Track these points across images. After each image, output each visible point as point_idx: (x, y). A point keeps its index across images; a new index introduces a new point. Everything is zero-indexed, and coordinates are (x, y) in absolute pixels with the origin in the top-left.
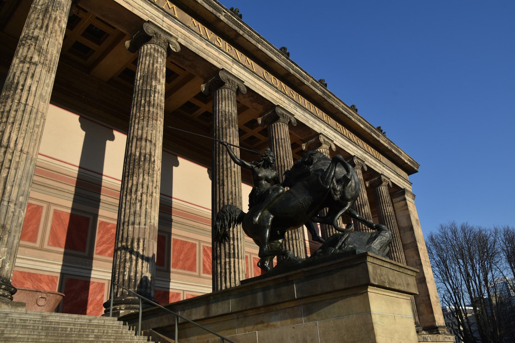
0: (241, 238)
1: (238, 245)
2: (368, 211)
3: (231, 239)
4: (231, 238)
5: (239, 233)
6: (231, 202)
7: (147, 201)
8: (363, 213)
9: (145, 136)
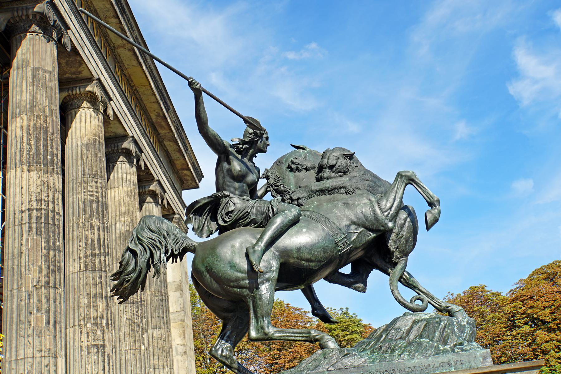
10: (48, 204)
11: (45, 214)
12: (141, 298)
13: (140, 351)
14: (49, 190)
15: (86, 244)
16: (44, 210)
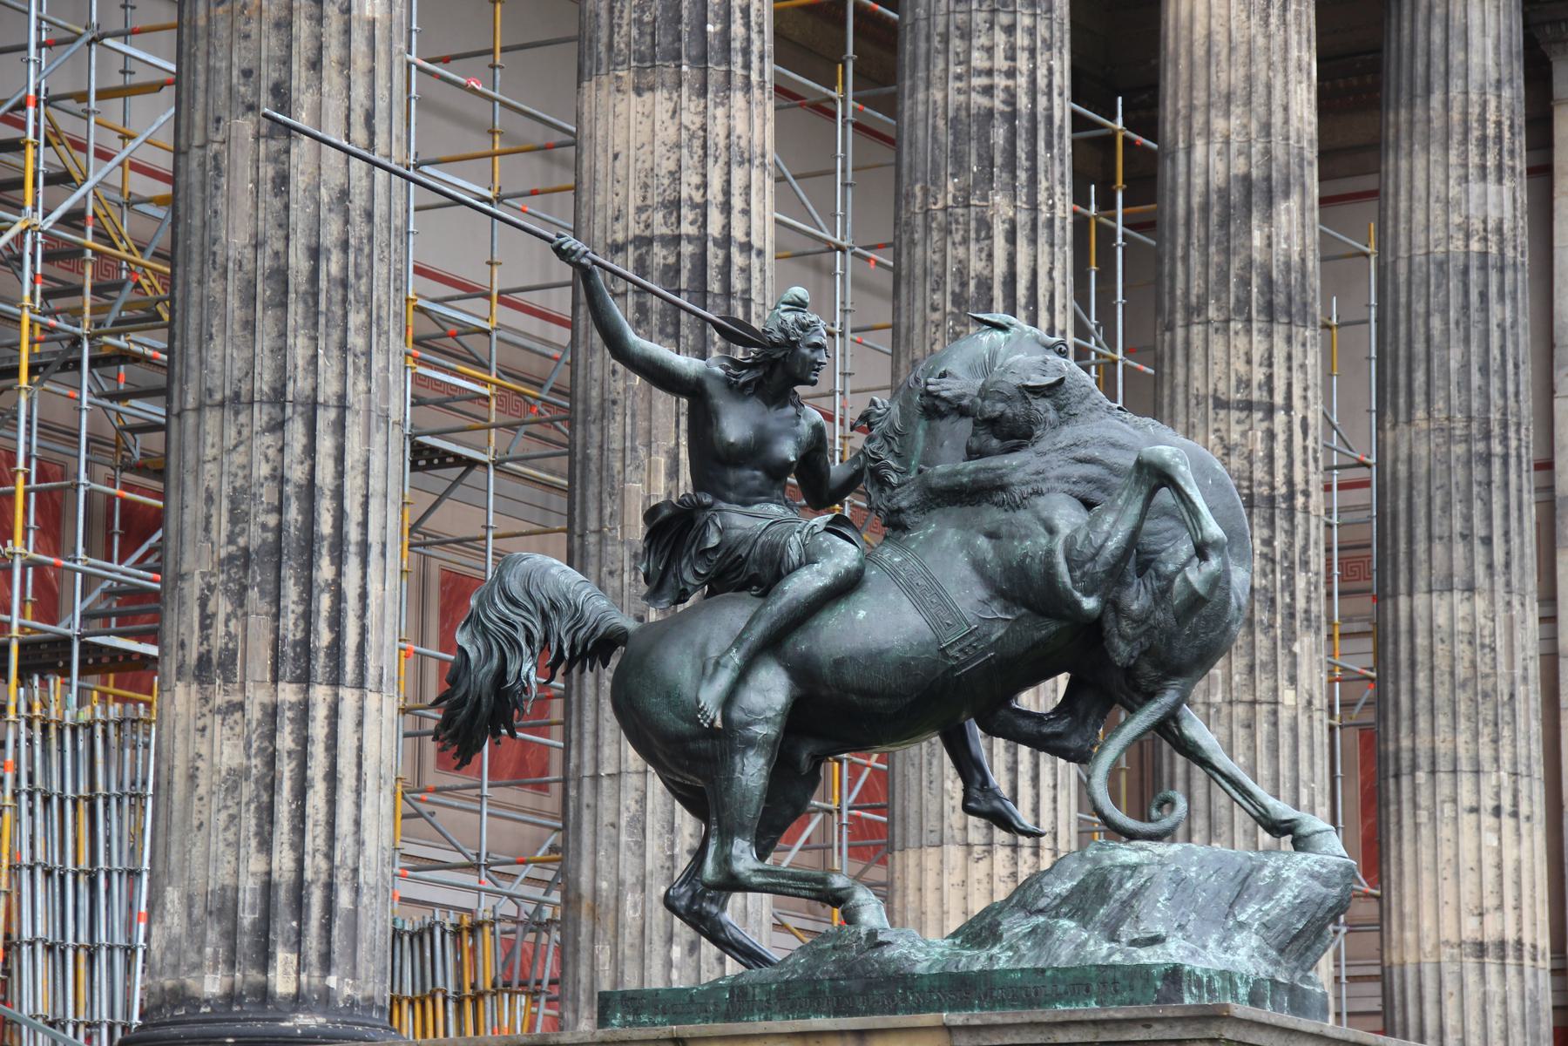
0: (384, 545)
1: (363, 596)
2: (1296, 248)
3: (325, 551)
4: (322, 538)
5: (374, 505)
6: (335, 269)
8: (1257, 256)
10: (705, 216)
11: (692, 256)
12: (1290, 482)
13: (1275, 713)
14: (710, 161)
15: (959, 300)
16: (690, 239)
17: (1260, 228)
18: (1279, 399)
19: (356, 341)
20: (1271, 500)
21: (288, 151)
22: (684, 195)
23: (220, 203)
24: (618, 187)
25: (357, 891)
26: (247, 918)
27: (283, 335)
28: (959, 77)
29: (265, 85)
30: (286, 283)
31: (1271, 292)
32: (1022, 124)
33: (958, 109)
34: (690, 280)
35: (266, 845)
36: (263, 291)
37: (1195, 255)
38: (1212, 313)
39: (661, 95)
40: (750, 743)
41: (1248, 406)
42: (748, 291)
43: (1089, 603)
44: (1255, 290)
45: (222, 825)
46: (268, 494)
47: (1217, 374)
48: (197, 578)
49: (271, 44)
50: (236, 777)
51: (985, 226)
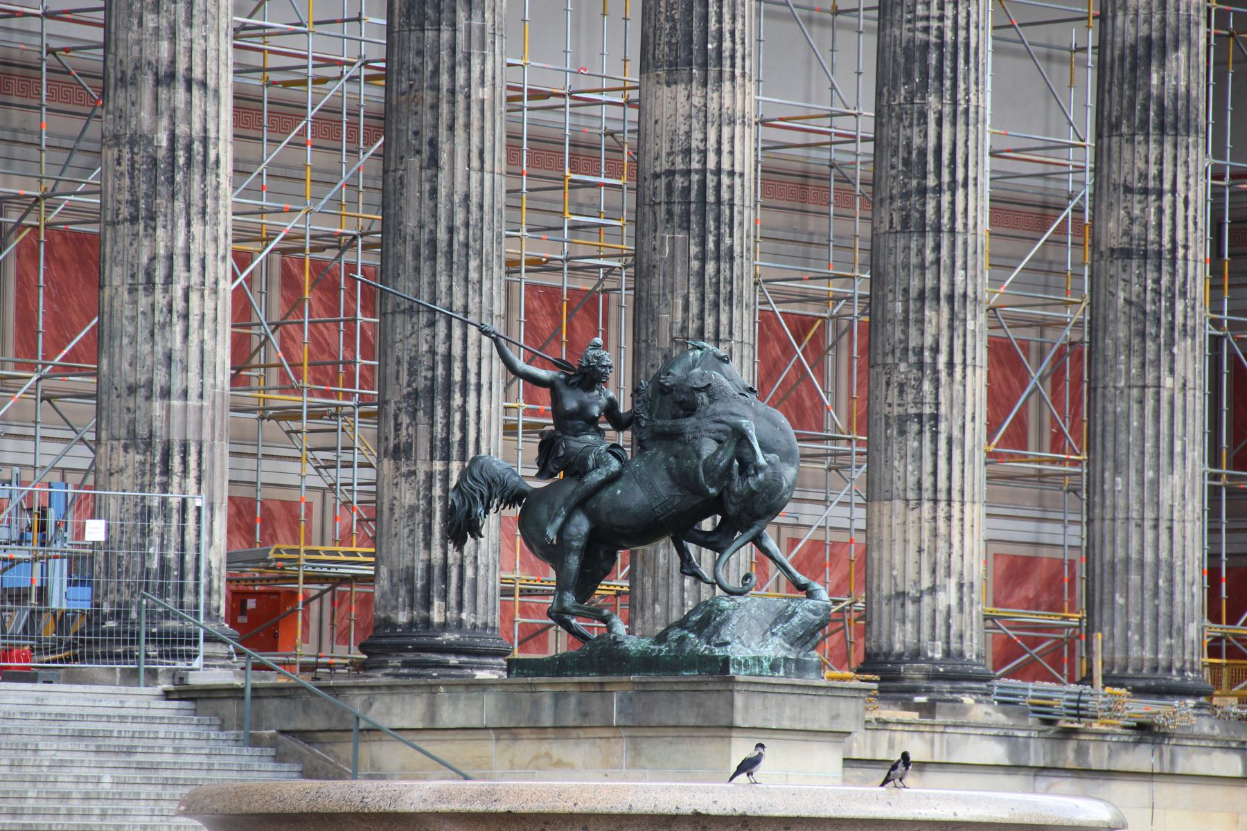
1: (479, 412)
2: (1183, 83)
6: (462, 237)
7: (203, 315)
8: (1154, 91)
9: (186, 66)
10: (705, 157)
11: (698, 181)
12: (1173, 240)
13: (1158, 393)
14: (709, 125)
15: (907, 162)
16: (697, 171)
17: (1158, 72)
18: (1167, 186)
19: (473, 275)
20: (1159, 254)
21: (436, 176)
22: (693, 146)
23: (403, 202)
24: (658, 140)
25: (476, 568)
26: (419, 584)
27: (434, 275)
28: (909, 21)
29: (426, 140)
30: (435, 246)
31: (1163, 115)
32: (948, 50)
33: (908, 41)
34: (697, 195)
35: (428, 546)
36: (425, 251)
37: (1115, 89)
38: (1124, 129)
39: (681, 87)
40: (571, 550)
41: (1145, 191)
42: (732, 199)
43: (712, 491)
44: (1152, 114)
45: (406, 535)
46: (426, 360)
47: (1126, 170)
48: (393, 404)
49: (428, 117)
50: (413, 509)
51: (923, 115)
